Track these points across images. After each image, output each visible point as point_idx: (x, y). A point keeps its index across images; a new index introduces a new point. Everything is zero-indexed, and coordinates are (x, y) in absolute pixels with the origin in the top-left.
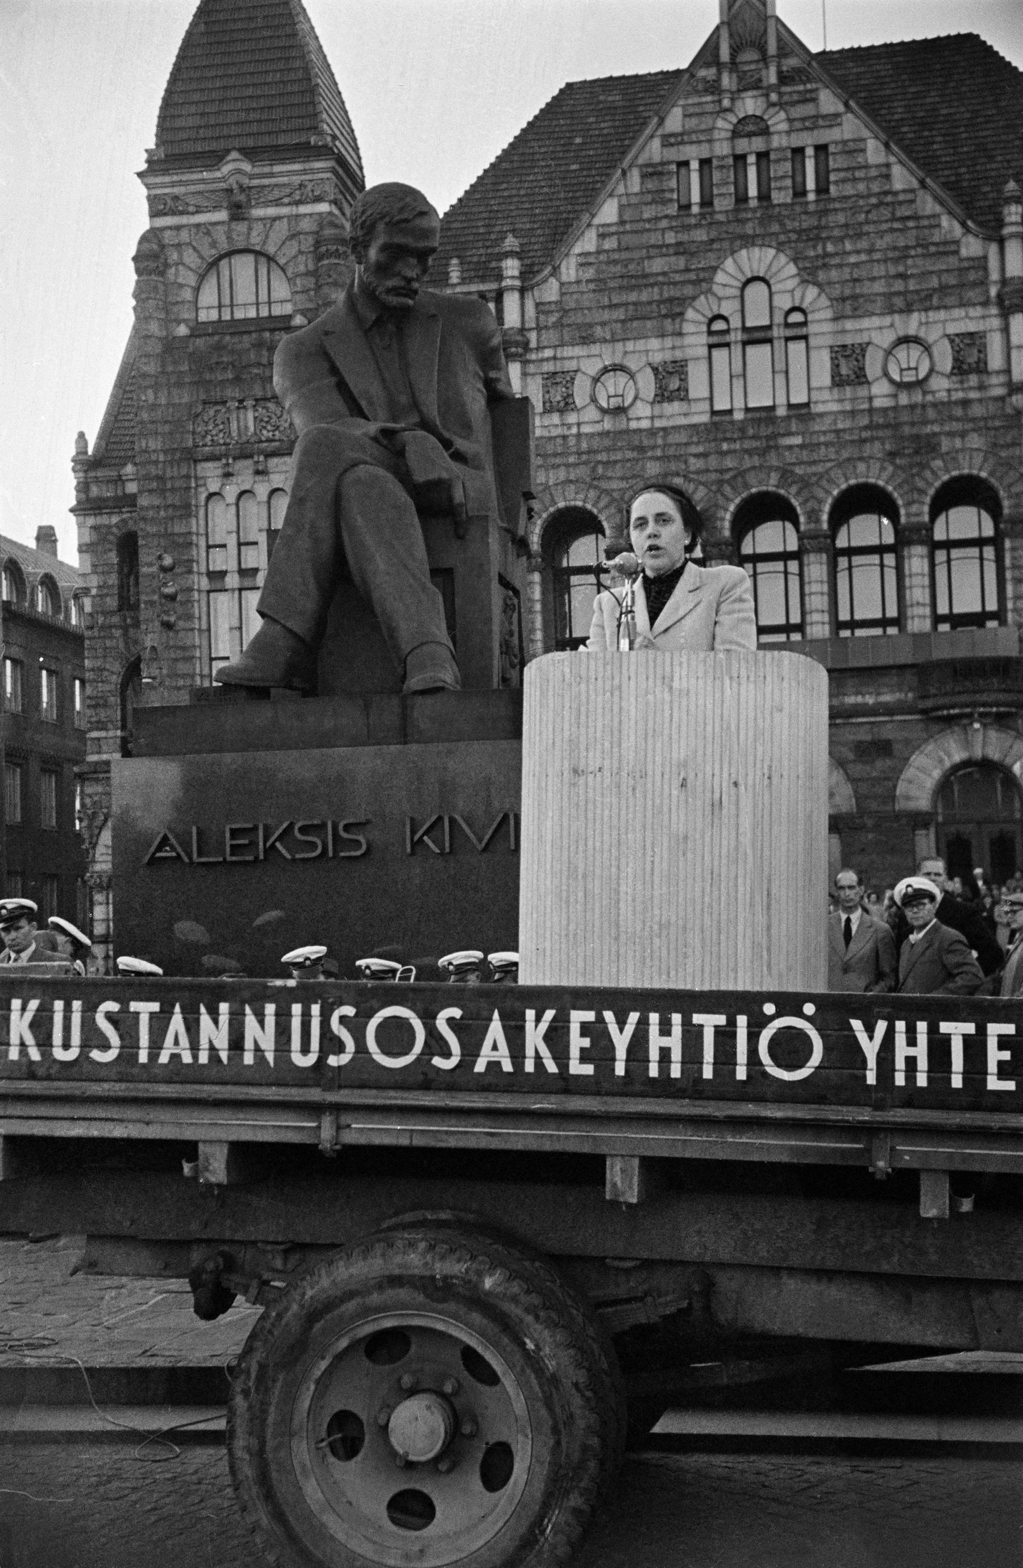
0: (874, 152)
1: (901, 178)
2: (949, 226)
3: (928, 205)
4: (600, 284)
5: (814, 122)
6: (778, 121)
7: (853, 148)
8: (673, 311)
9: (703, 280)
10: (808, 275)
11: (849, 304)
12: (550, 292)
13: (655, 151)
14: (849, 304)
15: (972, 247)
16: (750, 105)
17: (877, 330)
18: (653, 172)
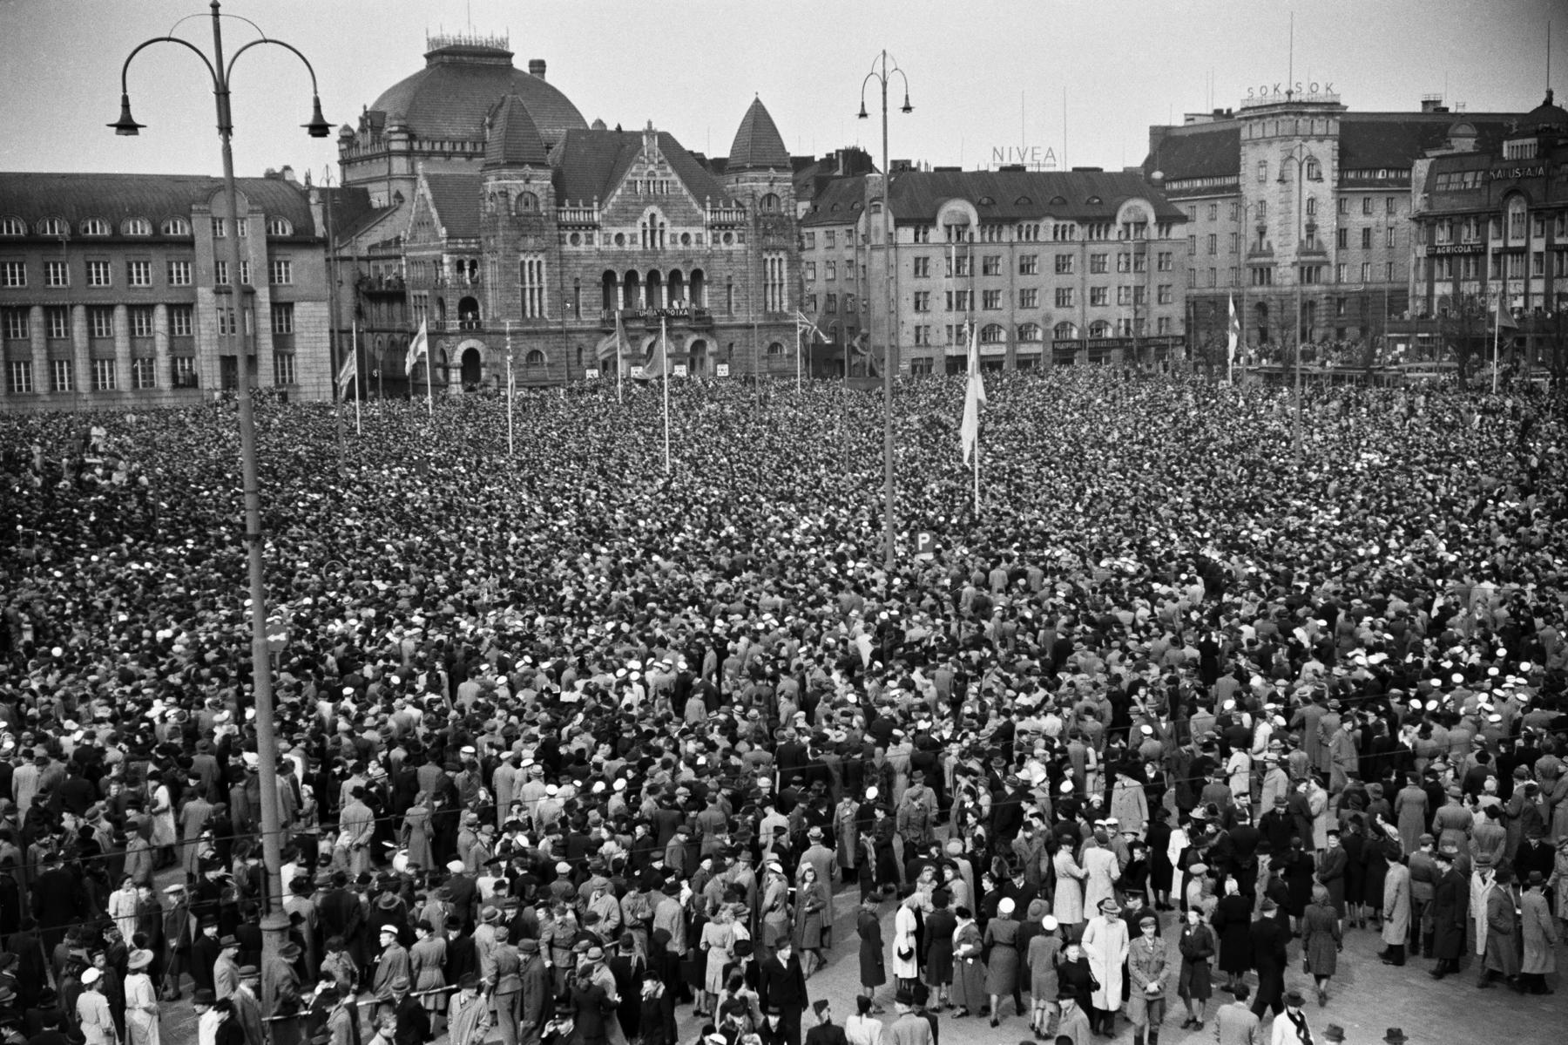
0: (679, 185)
1: (685, 192)
2: (695, 206)
3: (691, 199)
4: (617, 211)
5: (666, 175)
6: (658, 173)
7: (674, 183)
8: (634, 220)
9: (640, 213)
10: (666, 214)
11: (674, 223)
12: (605, 212)
13: (630, 177)
14: (674, 223)
15: (700, 211)
16: (652, 168)
17: (680, 231)
18: (629, 183)
